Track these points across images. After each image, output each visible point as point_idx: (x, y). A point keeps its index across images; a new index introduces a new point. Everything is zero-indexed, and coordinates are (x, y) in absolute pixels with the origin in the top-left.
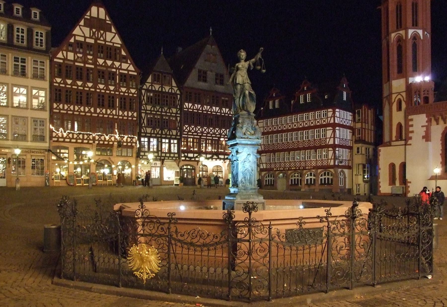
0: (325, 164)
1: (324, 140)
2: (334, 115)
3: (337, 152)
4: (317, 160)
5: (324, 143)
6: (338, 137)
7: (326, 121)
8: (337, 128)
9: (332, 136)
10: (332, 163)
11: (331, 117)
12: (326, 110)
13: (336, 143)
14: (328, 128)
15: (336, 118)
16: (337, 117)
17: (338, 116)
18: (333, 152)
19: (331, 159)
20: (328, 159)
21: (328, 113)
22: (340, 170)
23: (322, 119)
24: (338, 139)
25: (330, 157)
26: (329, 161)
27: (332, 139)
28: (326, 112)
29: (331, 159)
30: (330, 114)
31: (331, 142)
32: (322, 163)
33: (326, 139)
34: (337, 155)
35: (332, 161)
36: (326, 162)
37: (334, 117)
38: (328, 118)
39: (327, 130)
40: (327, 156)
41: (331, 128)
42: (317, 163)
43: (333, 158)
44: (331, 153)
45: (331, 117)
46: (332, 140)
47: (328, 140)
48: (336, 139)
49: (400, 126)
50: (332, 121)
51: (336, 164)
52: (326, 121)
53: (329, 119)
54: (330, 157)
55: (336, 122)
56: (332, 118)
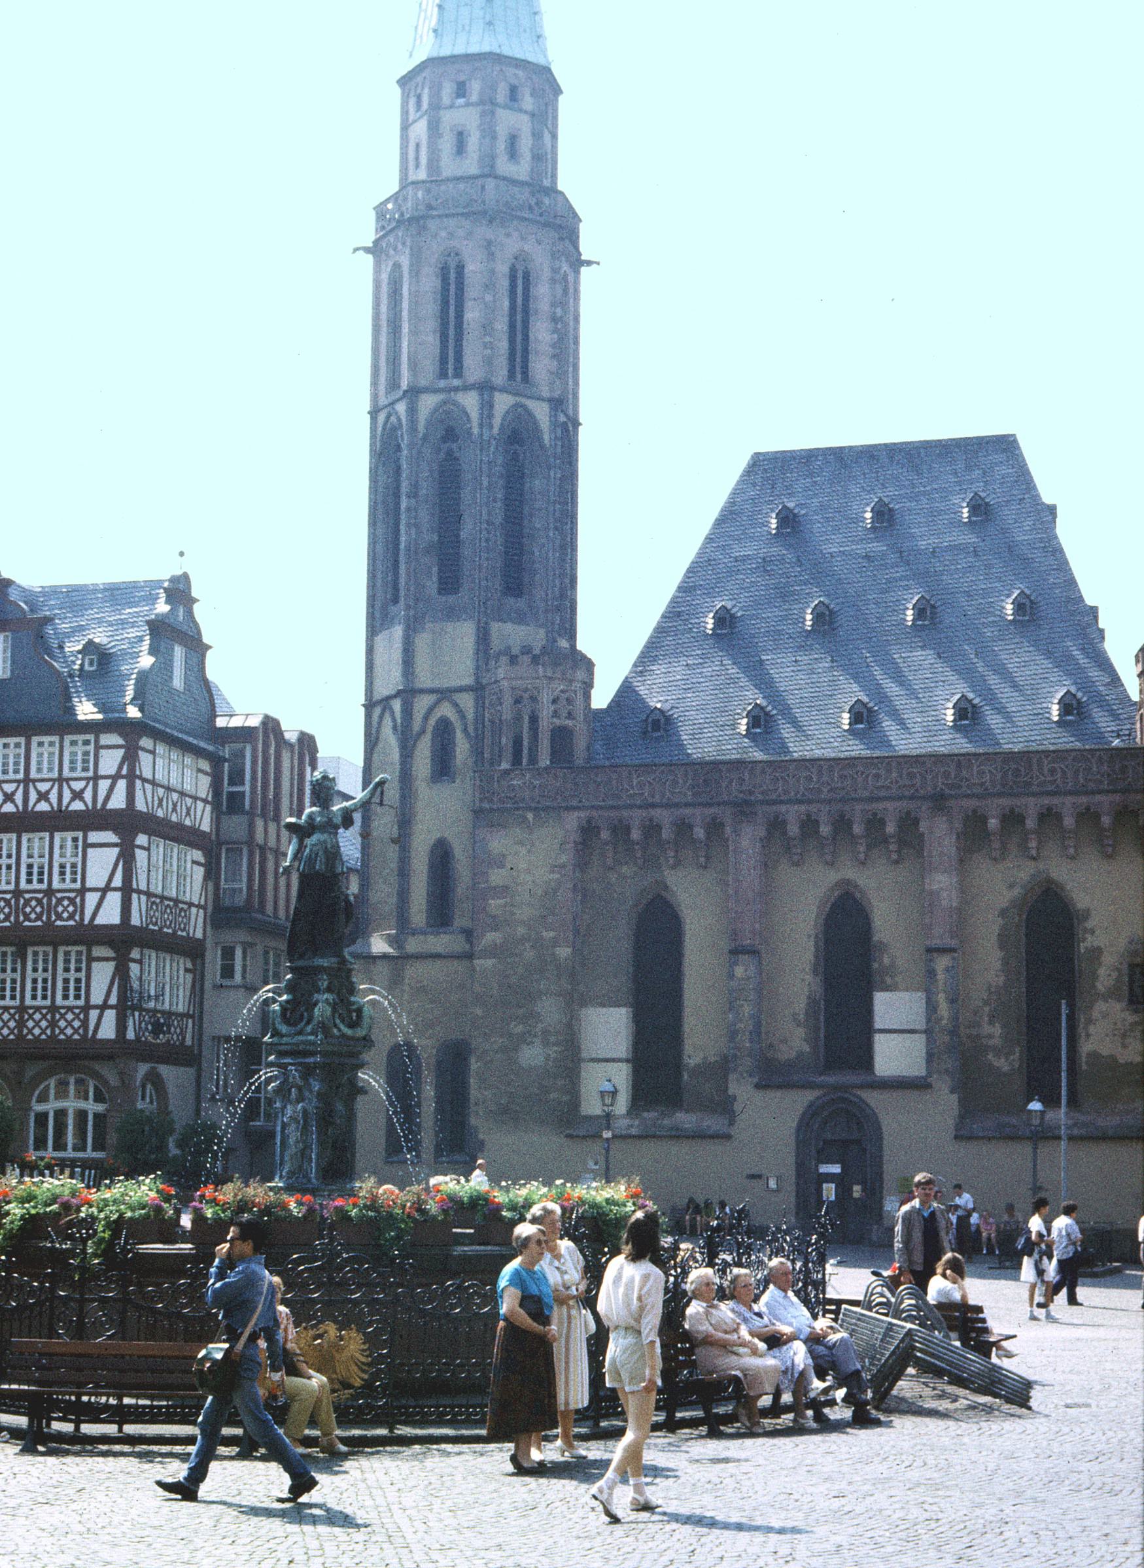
0: (68, 1028)
1: (72, 901)
2: (132, 769)
3: (134, 968)
4: (22, 1009)
5: (71, 917)
6: (143, 887)
7: (88, 795)
8: (142, 839)
9: (117, 881)
10: (108, 1031)
11: (115, 778)
12: (91, 737)
13: (135, 921)
14: (94, 837)
15: (138, 782)
16: (144, 780)
17: (148, 774)
18: (117, 968)
19: (104, 1007)
20: (87, 1008)
21: (102, 752)
22: (143, 1069)
23: (68, 780)
24: (143, 898)
25: (97, 998)
26: (94, 1014)
27: (114, 899)
28: (91, 748)
29: (104, 1007)
30: (110, 761)
31: (110, 915)
32: (53, 1024)
33: (83, 891)
34: (136, 985)
35: (110, 1015)
36: (76, 1024)
37: (131, 778)
38: (96, 778)
39: (87, 845)
40: (83, 987)
41: (109, 837)
42: (21, 1024)
43: (113, 1000)
44: (102, 974)
45: (115, 778)
46: (114, 900)
47: (92, 899)
48: (135, 896)
49: (442, 856)
50: (118, 801)
51: (130, 1035)
52: (88, 795)
53: (104, 785)
54: (97, 998)
55: (140, 805)
56: (122, 784)
